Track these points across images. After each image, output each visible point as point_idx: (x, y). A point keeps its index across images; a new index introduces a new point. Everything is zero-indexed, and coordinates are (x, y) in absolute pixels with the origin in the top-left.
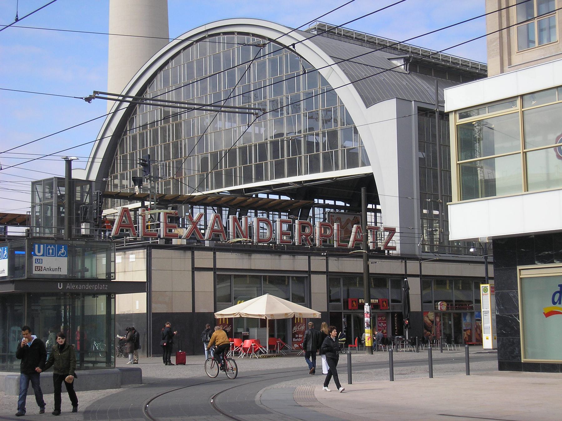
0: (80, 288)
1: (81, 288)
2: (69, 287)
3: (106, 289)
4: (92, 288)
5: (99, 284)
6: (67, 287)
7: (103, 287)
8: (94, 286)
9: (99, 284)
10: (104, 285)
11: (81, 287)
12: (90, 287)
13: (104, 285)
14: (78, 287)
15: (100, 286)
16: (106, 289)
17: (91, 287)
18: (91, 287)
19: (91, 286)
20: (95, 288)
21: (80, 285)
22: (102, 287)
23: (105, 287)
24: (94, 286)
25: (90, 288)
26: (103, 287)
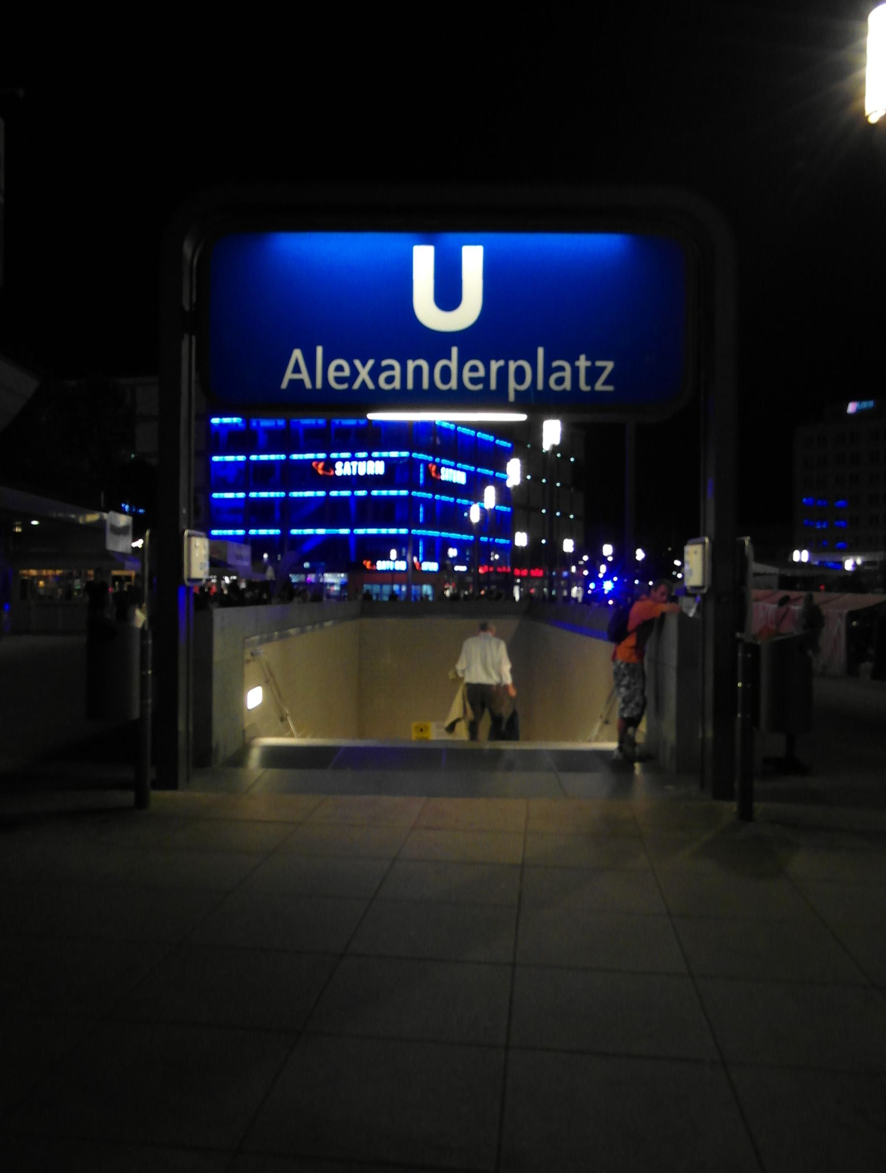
0: (389, 380)
1: (397, 384)
2: (304, 375)
3: (599, 386)
4: (486, 380)
5: (541, 351)
6: (289, 375)
7: (575, 371)
8: (503, 373)
9: (541, 351)
10: (583, 363)
11: (397, 373)
12: (467, 374)
13: (583, 363)
14: (374, 374)
15: (548, 371)
16: (599, 386)
17: (481, 373)
18: (481, 373)
19: (474, 369)
20: (512, 384)
21: (385, 363)
22: (567, 374)
23: (593, 374)
24: (503, 373)
25: (473, 381)
26: (575, 371)
